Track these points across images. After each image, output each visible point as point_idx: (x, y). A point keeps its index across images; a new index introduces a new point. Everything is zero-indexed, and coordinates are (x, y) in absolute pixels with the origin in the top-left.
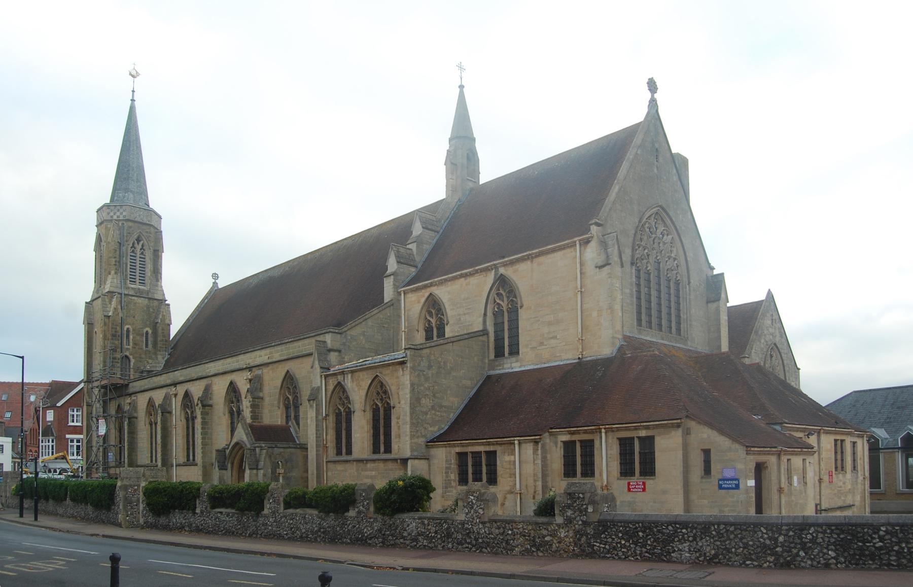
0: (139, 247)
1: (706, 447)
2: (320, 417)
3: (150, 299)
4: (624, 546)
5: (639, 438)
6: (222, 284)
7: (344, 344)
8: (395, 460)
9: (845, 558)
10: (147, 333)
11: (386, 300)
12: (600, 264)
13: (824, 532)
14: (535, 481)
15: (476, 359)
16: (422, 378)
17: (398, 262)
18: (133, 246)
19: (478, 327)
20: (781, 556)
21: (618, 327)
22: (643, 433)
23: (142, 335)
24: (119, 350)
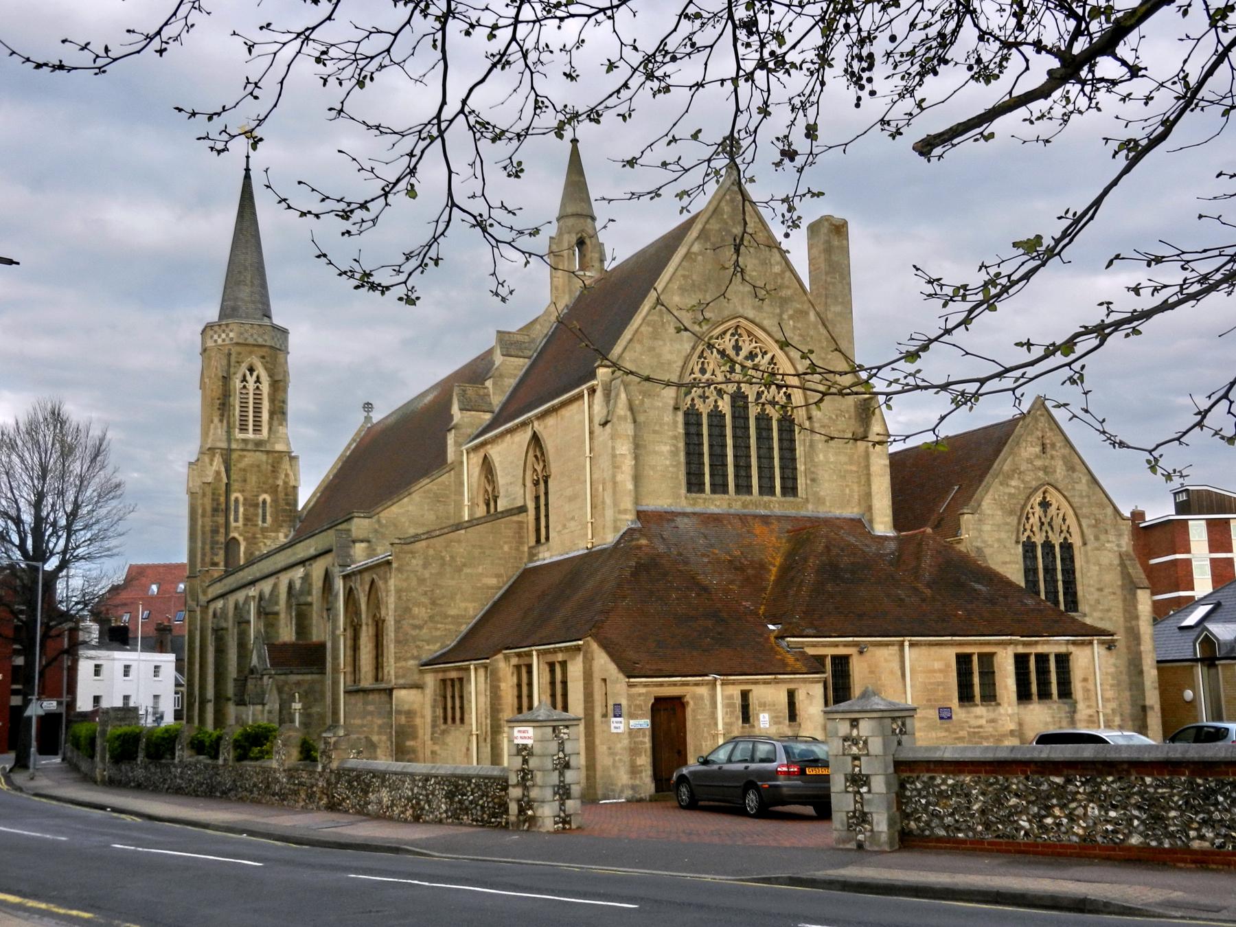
0: (251, 380)
3: (268, 452)
6: (377, 417)
8: (385, 690)
11: (449, 461)
12: (603, 421)
15: (506, 548)
16: (414, 583)
17: (461, 410)
19: (520, 503)
21: (627, 503)
22: (560, 657)
24: (222, 530)
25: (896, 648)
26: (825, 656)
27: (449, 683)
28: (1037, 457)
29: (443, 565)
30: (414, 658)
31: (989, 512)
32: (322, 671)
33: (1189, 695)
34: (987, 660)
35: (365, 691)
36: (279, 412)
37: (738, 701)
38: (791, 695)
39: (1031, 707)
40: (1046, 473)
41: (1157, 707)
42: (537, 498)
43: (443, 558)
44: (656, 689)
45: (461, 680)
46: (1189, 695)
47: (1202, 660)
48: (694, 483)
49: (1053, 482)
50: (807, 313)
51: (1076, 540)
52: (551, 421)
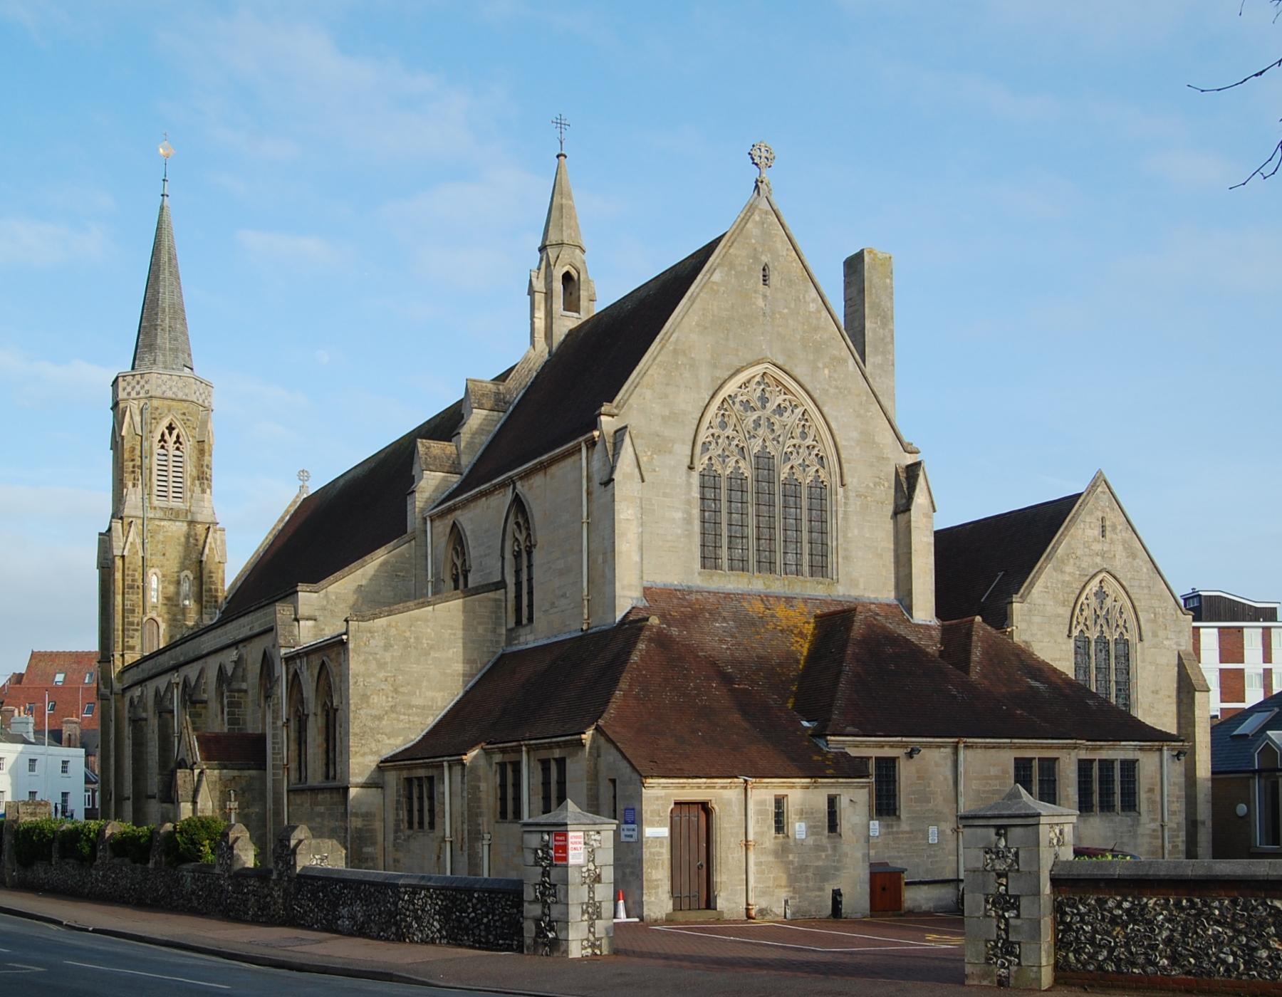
2: (280, 723)
4: (312, 911)
6: (313, 488)
7: (324, 608)
8: (337, 789)
12: (605, 479)
15: (480, 630)
16: (373, 666)
18: (163, 439)
22: (557, 753)
25: (948, 750)
26: (869, 758)
27: (416, 782)
28: (1095, 540)
29: (406, 647)
30: (372, 753)
31: (1040, 601)
32: (262, 766)
33: (1242, 809)
34: (1049, 766)
35: (314, 790)
36: (203, 478)
37: (771, 808)
38: (832, 801)
39: (1091, 819)
41: (1209, 823)
42: (518, 572)
44: (676, 791)
45: (431, 779)
46: (1242, 809)
47: (1259, 771)
48: (709, 560)
49: (1109, 568)
51: (1132, 636)
52: (538, 480)
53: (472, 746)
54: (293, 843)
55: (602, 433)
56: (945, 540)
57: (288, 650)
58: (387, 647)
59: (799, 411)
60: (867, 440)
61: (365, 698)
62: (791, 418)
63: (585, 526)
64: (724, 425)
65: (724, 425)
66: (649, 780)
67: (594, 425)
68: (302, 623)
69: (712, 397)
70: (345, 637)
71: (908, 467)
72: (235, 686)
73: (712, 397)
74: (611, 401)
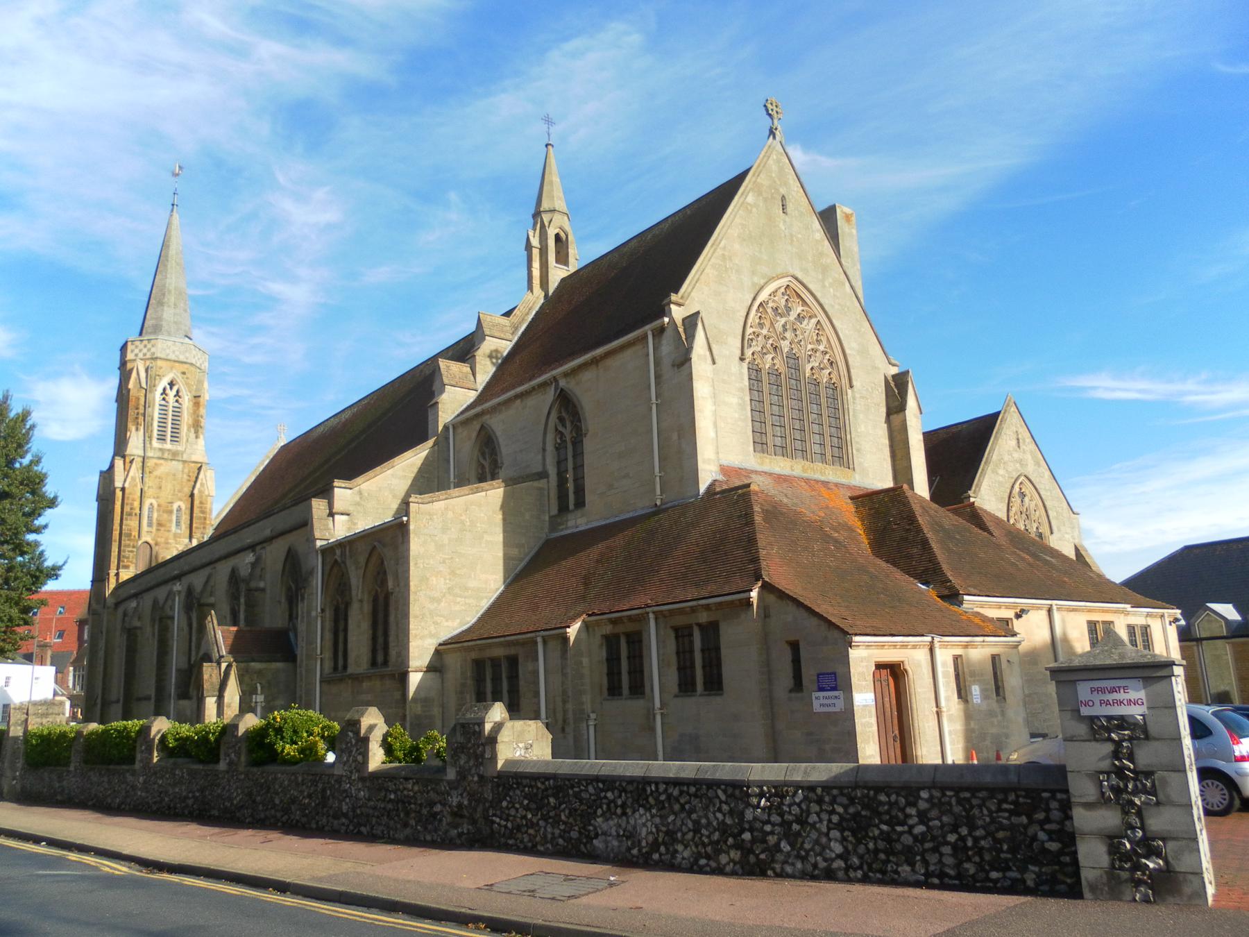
1: (792, 638)
4: (531, 825)
5: (699, 625)
8: (392, 676)
9: (861, 857)
10: (179, 509)
13: (820, 801)
14: (564, 702)
15: (527, 516)
20: (751, 851)
22: (704, 618)
23: (171, 512)
30: (432, 636)
40: (1022, 465)
42: (560, 463)
43: (462, 522)
48: (760, 444)
50: (843, 284)
52: (587, 376)
53: (573, 619)
54: (488, 727)
55: (672, 320)
56: (929, 437)
57: (324, 543)
58: (445, 530)
59: (814, 321)
60: (863, 351)
61: (424, 579)
62: (809, 325)
63: (654, 407)
64: (761, 325)
65: (761, 325)
66: (856, 639)
67: (663, 311)
68: (336, 517)
69: (754, 299)
70: (405, 519)
71: (894, 376)
72: (253, 585)
73: (754, 299)
74: (676, 292)
